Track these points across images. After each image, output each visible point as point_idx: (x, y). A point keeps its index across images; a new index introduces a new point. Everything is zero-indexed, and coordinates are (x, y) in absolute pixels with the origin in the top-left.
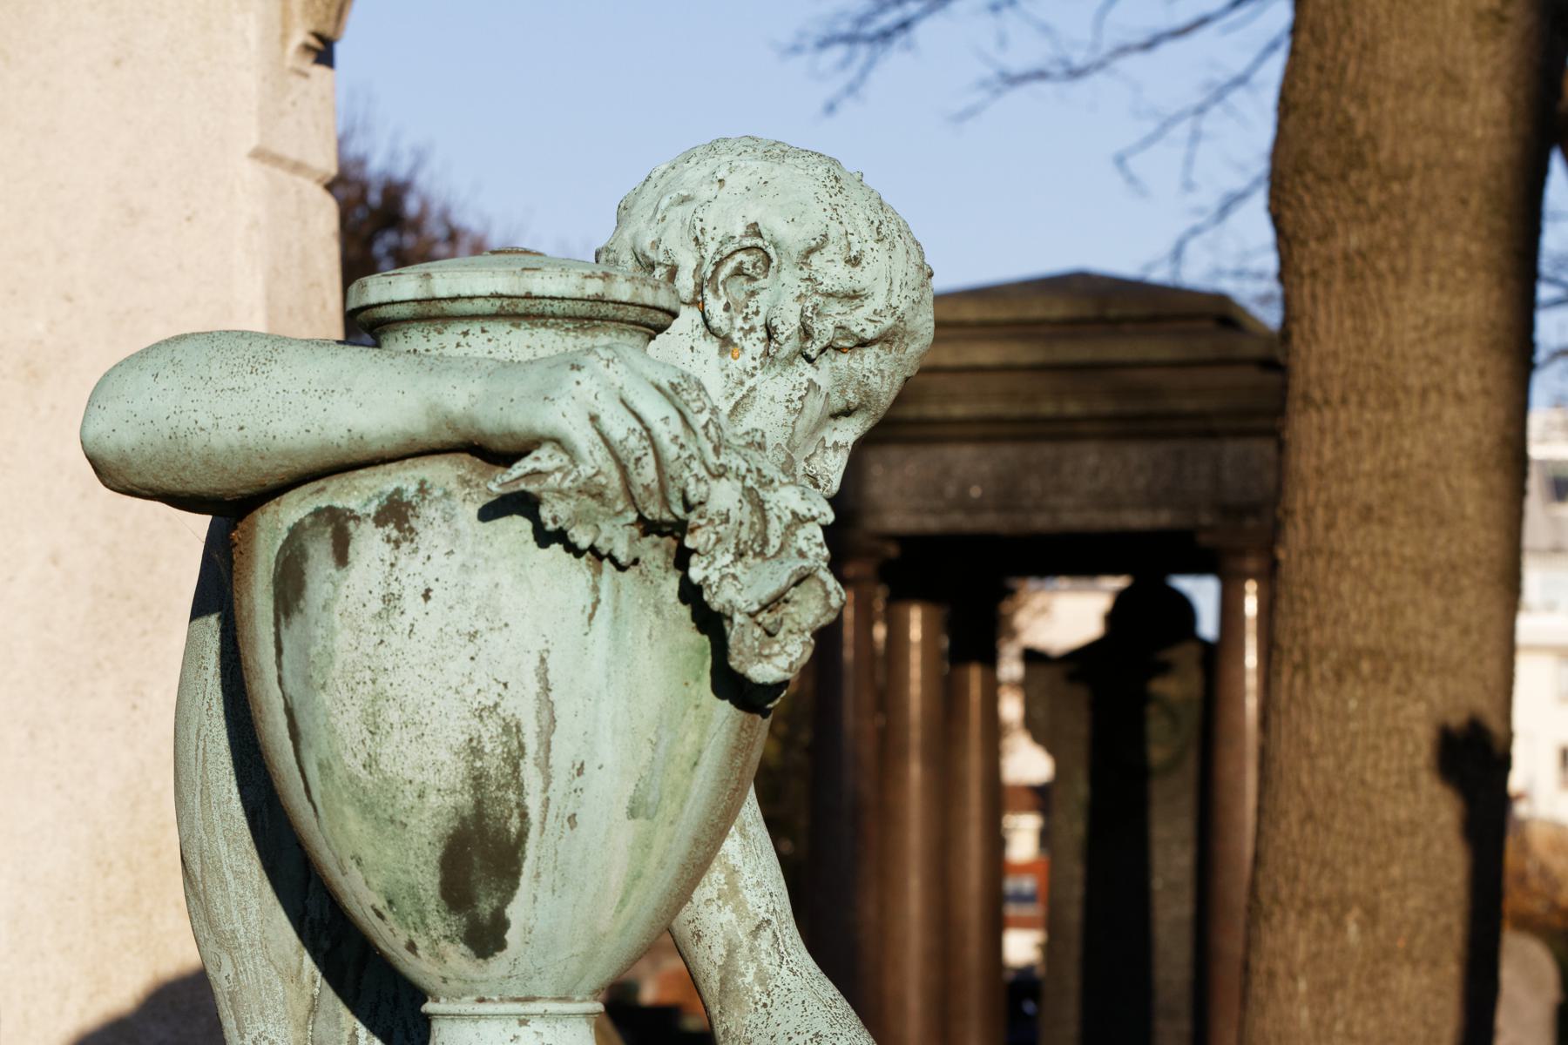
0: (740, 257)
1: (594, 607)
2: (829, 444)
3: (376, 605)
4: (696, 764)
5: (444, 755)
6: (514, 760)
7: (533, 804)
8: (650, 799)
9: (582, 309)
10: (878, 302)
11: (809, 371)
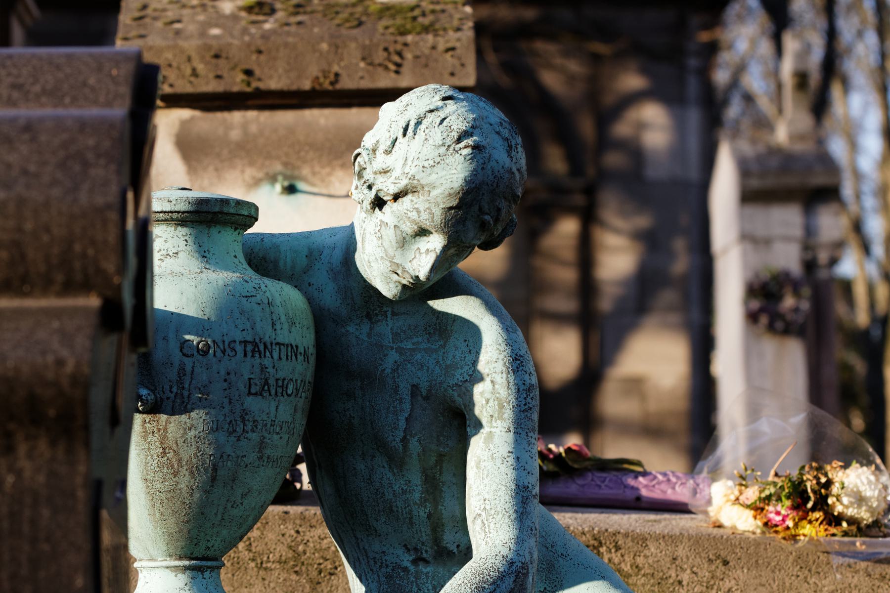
2: (423, 250)
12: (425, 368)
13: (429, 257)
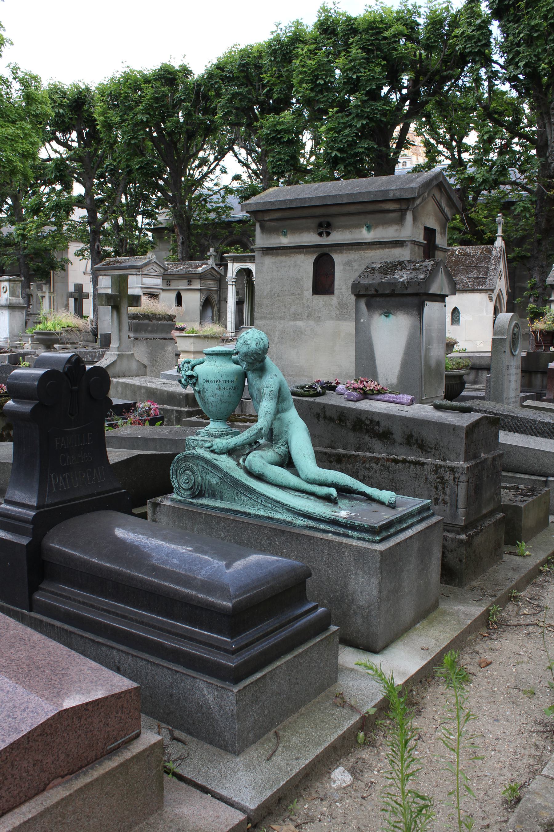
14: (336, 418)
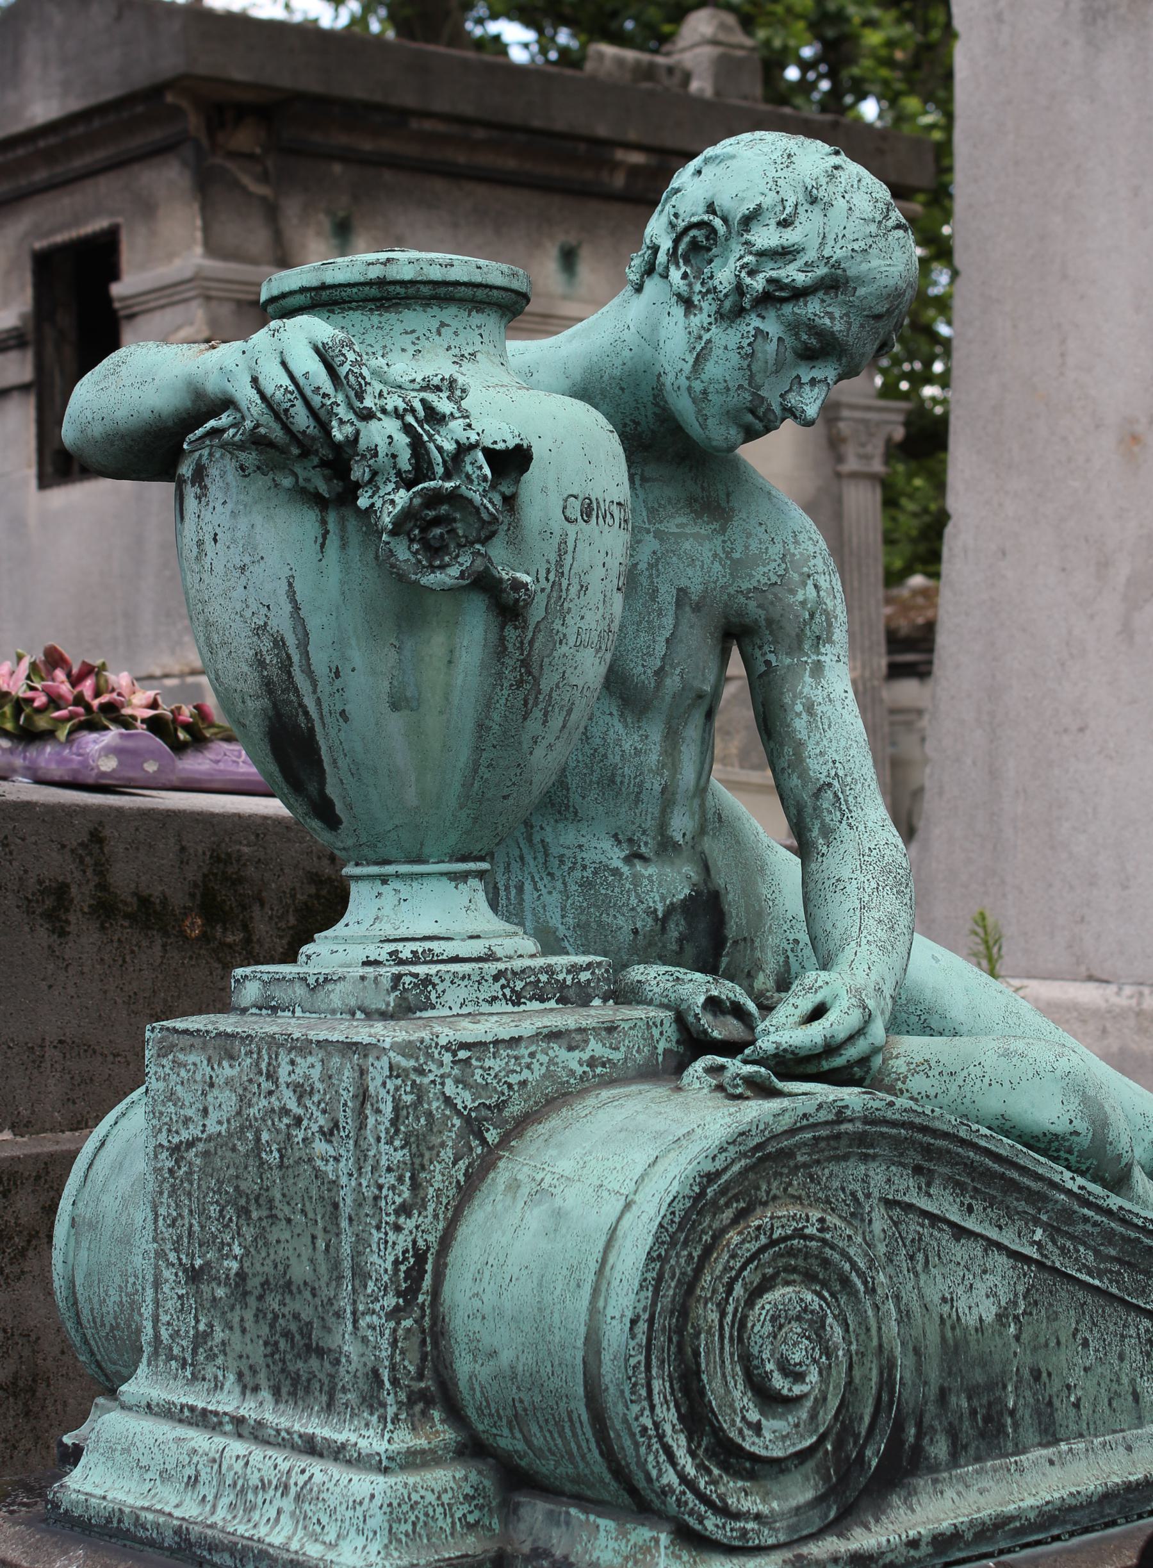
0: (693, 232)
1: (324, 537)
3: (195, 550)
4: (450, 662)
5: (245, 668)
6: (286, 665)
7: (309, 702)
8: (409, 694)
9: (374, 292)
10: (811, 255)
11: (756, 322)
12: (698, 563)
13: (816, 390)
14: (179, 899)
